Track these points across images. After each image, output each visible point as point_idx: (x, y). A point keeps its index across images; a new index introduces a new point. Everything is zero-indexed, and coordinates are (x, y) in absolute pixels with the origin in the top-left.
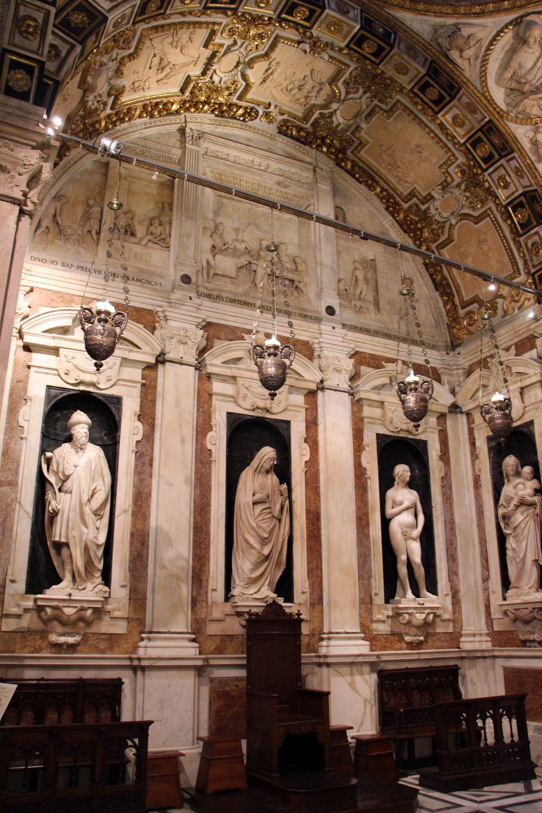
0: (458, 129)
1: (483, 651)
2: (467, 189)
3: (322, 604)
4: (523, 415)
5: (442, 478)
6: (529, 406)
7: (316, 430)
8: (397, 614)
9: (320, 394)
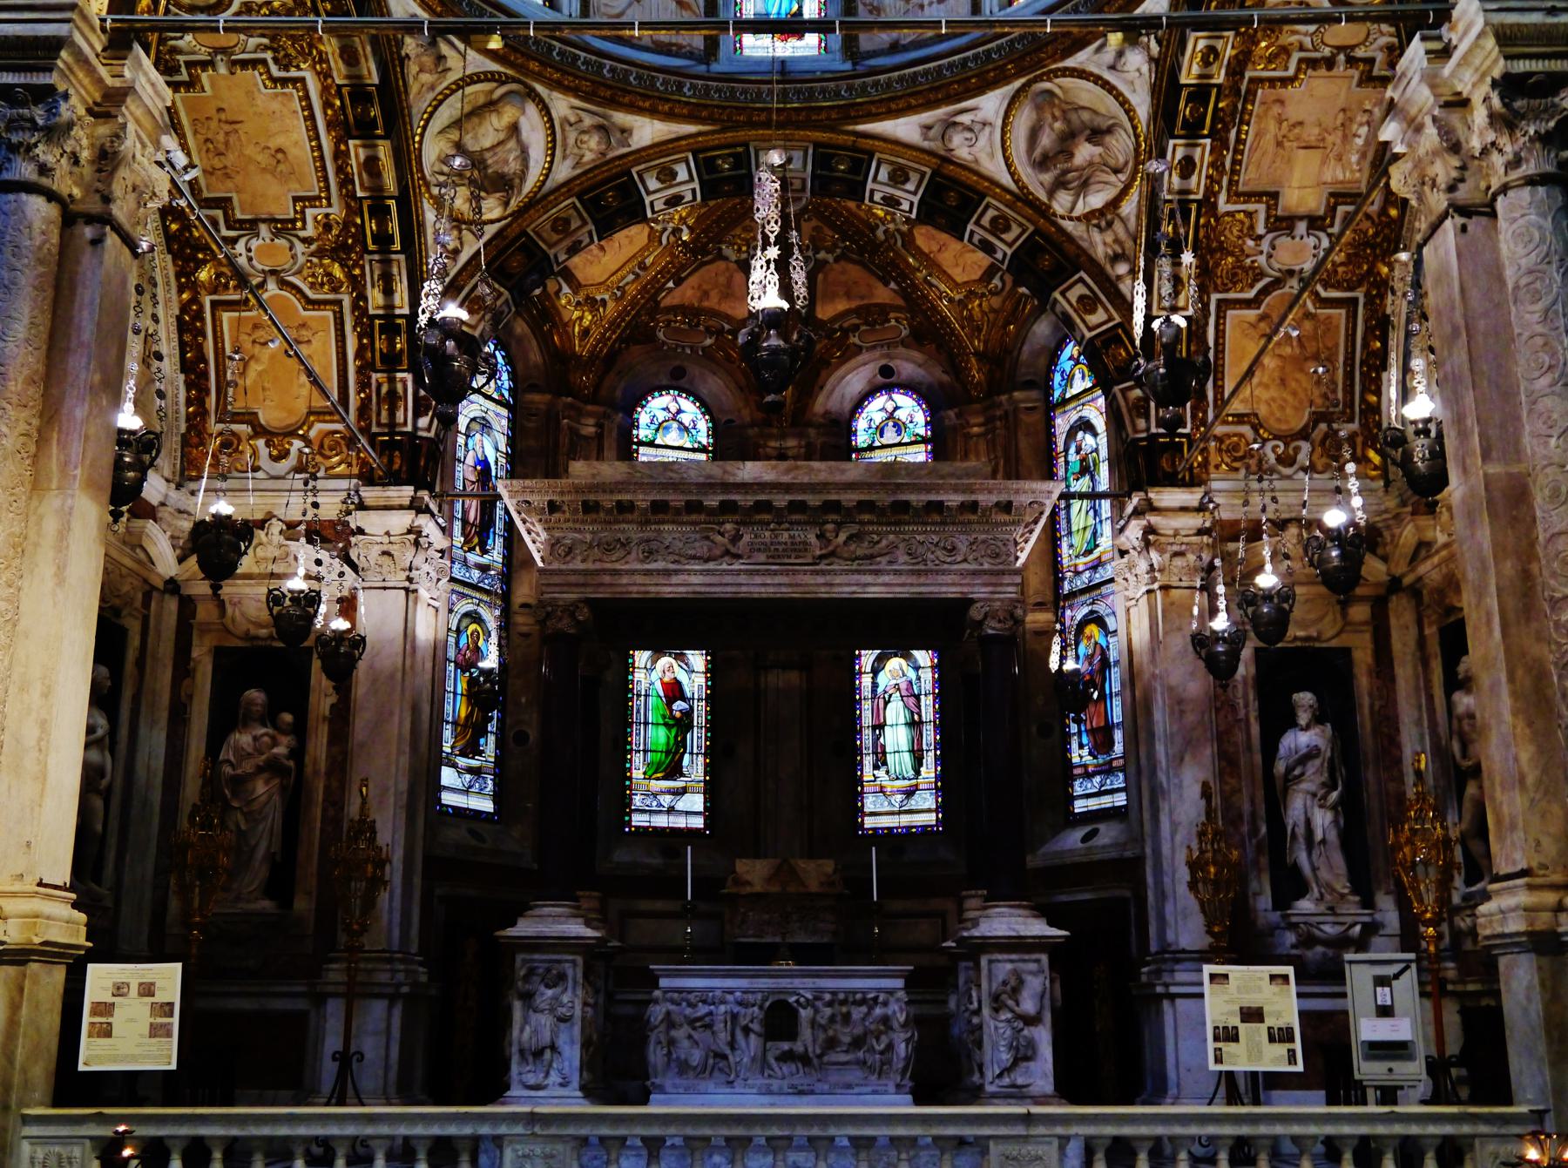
0: (365, 175)
2: (320, 253)
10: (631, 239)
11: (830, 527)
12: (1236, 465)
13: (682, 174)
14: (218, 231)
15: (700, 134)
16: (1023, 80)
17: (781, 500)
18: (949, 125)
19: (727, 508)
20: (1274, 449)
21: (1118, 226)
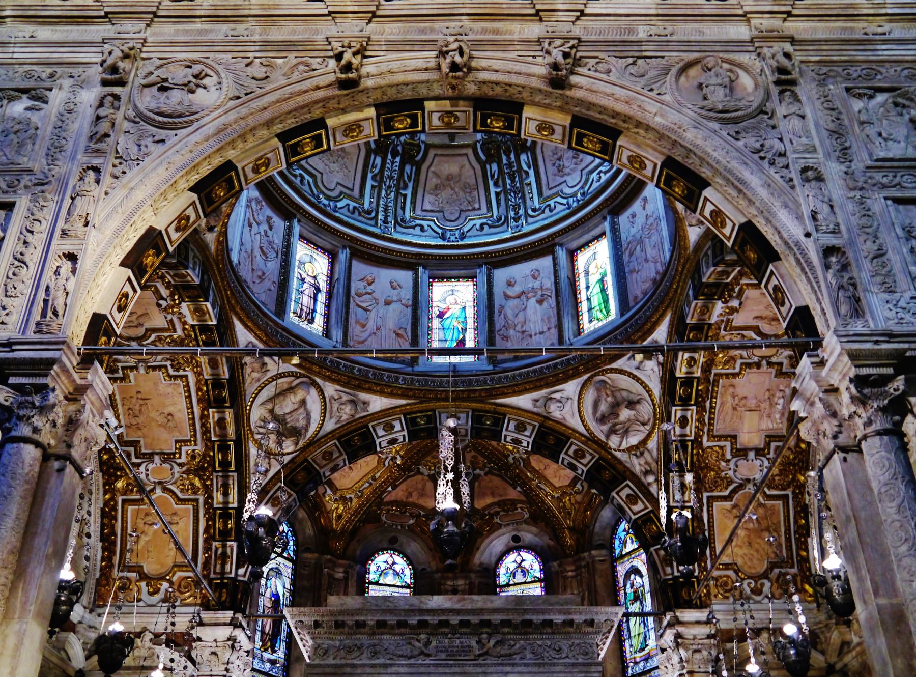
0: (217, 428)
2: (188, 472)
10: (367, 463)
11: (485, 636)
12: (727, 594)
13: (398, 427)
14: (130, 459)
15: (408, 404)
16: (588, 375)
17: (454, 620)
18: (549, 399)
19: (422, 624)
20: (749, 584)
21: (646, 454)
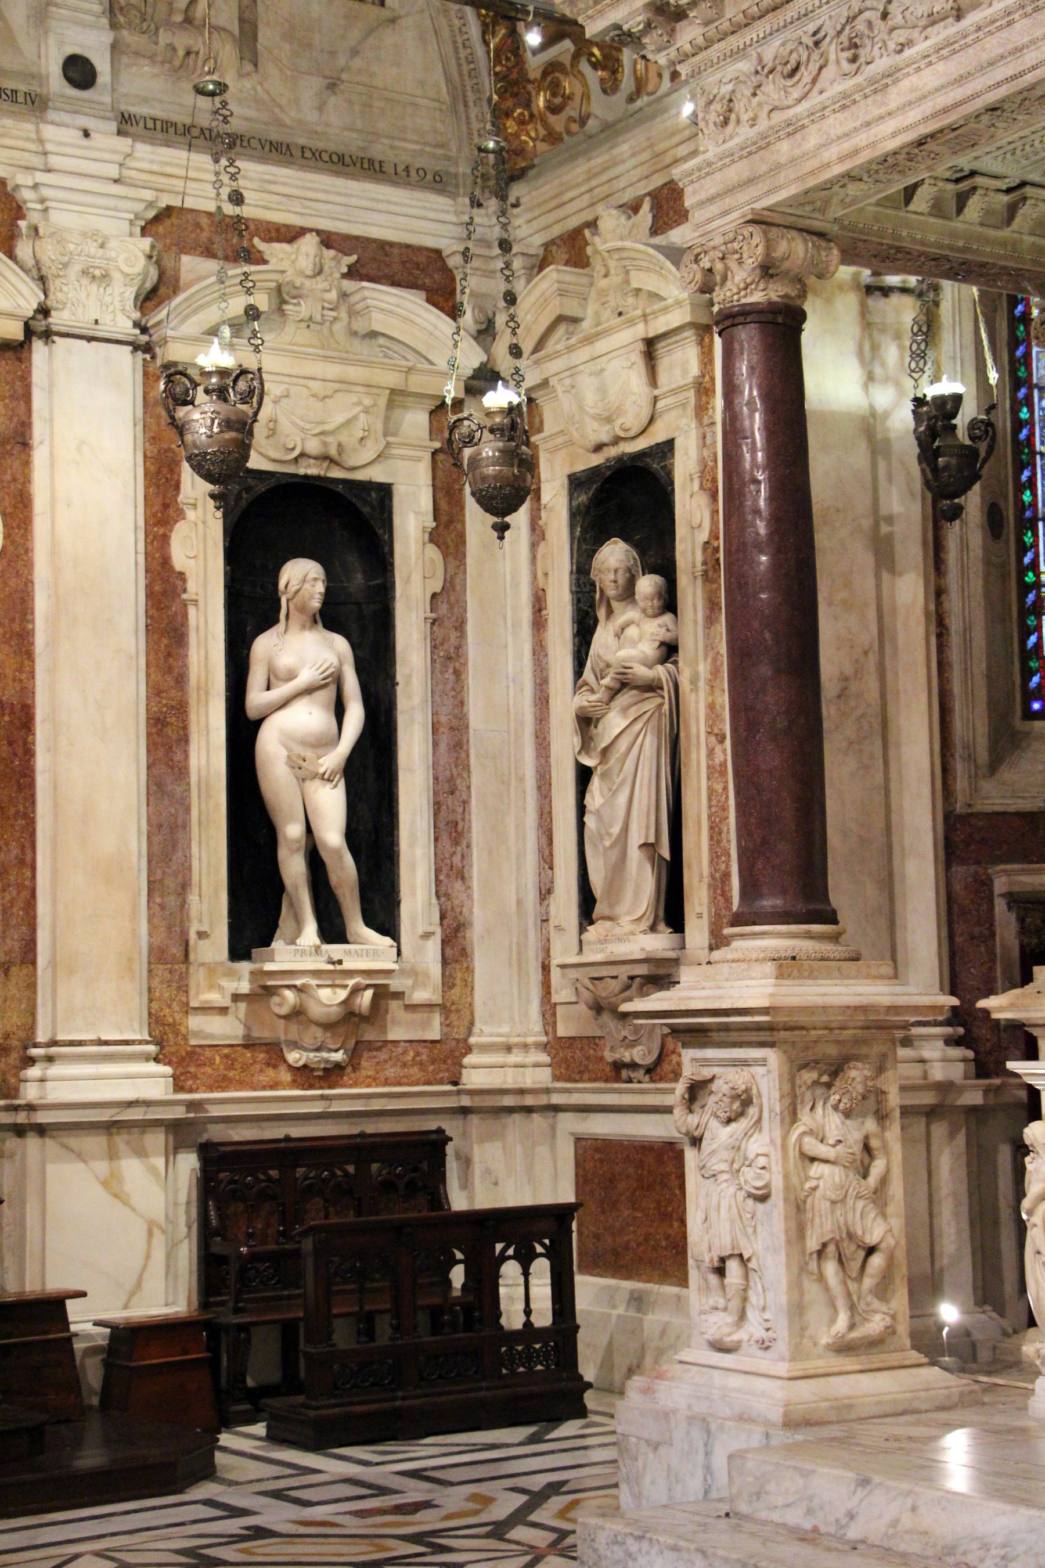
1: (521, 1092)
3: (34, 963)
4: (652, 420)
5: (434, 596)
6: (665, 396)
7: (27, 463)
8: (264, 992)
9: (39, 349)
